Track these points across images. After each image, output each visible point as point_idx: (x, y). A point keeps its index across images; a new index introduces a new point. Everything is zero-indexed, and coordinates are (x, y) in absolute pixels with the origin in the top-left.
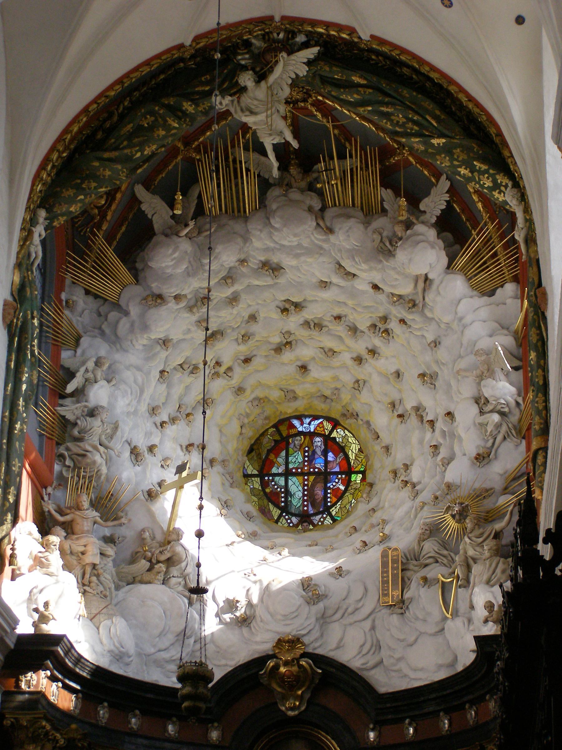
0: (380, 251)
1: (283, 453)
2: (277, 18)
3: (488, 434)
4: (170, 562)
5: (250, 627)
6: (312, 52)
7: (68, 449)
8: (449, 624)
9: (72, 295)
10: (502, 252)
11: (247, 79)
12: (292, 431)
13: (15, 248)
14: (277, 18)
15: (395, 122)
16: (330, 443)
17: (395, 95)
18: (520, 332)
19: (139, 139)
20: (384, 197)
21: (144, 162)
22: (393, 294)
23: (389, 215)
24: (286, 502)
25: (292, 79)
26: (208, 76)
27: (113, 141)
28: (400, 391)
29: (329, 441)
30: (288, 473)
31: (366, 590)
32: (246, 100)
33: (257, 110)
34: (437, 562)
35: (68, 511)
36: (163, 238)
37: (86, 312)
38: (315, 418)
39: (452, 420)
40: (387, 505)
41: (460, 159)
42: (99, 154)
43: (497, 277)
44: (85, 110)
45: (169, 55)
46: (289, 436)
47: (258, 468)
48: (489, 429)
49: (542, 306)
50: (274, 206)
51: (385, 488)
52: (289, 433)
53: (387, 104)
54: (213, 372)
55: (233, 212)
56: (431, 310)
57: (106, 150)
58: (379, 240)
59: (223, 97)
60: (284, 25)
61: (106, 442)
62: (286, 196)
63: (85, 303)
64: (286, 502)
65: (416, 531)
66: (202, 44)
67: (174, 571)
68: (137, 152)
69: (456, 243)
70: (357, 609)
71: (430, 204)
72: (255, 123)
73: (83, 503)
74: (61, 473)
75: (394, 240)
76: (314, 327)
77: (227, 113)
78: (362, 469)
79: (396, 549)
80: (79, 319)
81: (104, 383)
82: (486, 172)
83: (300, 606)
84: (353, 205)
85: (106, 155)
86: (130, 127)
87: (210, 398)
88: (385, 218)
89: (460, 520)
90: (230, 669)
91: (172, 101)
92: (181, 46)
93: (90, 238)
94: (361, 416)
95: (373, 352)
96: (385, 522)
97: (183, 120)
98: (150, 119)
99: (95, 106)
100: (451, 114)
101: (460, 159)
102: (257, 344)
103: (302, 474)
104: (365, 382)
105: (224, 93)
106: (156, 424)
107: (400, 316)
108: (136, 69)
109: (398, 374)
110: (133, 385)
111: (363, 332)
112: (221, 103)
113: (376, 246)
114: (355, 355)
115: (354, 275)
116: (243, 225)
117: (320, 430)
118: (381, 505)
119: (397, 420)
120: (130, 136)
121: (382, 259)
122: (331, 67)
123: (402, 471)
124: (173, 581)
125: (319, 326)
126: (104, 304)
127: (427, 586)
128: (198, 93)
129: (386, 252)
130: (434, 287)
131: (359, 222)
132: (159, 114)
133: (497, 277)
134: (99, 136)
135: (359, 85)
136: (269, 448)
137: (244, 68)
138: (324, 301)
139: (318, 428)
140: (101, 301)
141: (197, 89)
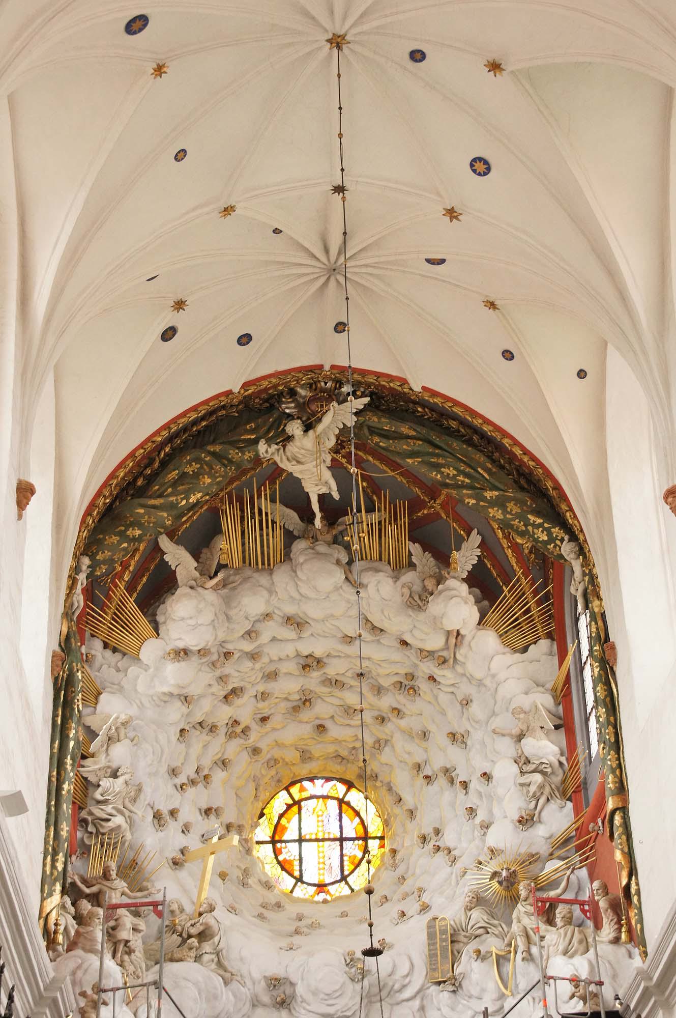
0: (409, 606)
3: (531, 794)
7: (90, 813)
9: (91, 649)
10: (535, 608)
11: (295, 428)
12: (305, 795)
13: (63, 597)
15: (445, 474)
16: (344, 807)
17: (446, 448)
18: (558, 691)
19: (184, 487)
20: (412, 551)
21: (189, 510)
22: (421, 650)
23: (418, 569)
24: (301, 871)
26: (253, 424)
27: (157, 487)
28: (426, 750)
30: (301, 840)
31: (412, 965)
32: (291, 448)
33: (303, 460)
36: (188, 590)
37: (105, 667)
38: (328, 779)
39: (488, 781)
40: (418, 871)
41: (514, 512)
42: (142, 501)
43: (529, 634)
44: (132, 455)
45: (217, 402)
47: (271, 834)
48: (533, 789)
49: (612, 659)
50: (301, 559)
51: (412, 854)
53: (438, 456)
54: (230, 730)
55: (257, 564)
57: (151, 497)
58: (408, 595)
59: (269, 446)
60: (334, 374)
61: (129, 805)
62: (313, 549)
64: (301, 871)
65: (462, 900)
67: (207, 947)
68: (182, 500)
69: (484, 599)
71: (461, 559)
72: (301, 472)
73: (111, 872)
74: (82, 839)
76: (335, 684)
78: (379, 835)
79: (444, 919)
80: (97, 673)
81: (127, 741)
82: (541, 525)
83: (344, 983)
84: (381, 559)
85: (152, 502)
86: (174, 474)
87: (227, 759)
88: (414, 572)
89: (508, 887)
91: (218, 448)
92: (229, 393)
93: (110, 589)
94: (380, 778)
95: (397, 711)
96: (421, 890)
97: (229, 468)
99: (142, 451)
100: (502, 467)
101: (514, 512)
103: (317, 840)
104: (386, 741)
105: (269, 442)
106: (176, 786)
109: (425, 735)
110: (155, 744)
112: (267, 452)
113: (405, 600)
114: (376, 713)
115: (382, 630)
116: (268, 578)
117: (333, 794)
118: (410, 873)
119: (420, 781)
120: (175, 484)
121: (411, 613)
122: (379, 418)
123: (432, 835)
124: (206, 958)
126: (123, 658)
127: (479, 960)
129: (415, 607)
131: (388, 577)
132: (205, 462)
133: (529, 634)
134: (140, 482)
135: (408, 437)
136: (281, 812)
137: (290, 417)
138: (348, 656)
139: (331, 791)
140: (118, 656)
141: (242, 437)
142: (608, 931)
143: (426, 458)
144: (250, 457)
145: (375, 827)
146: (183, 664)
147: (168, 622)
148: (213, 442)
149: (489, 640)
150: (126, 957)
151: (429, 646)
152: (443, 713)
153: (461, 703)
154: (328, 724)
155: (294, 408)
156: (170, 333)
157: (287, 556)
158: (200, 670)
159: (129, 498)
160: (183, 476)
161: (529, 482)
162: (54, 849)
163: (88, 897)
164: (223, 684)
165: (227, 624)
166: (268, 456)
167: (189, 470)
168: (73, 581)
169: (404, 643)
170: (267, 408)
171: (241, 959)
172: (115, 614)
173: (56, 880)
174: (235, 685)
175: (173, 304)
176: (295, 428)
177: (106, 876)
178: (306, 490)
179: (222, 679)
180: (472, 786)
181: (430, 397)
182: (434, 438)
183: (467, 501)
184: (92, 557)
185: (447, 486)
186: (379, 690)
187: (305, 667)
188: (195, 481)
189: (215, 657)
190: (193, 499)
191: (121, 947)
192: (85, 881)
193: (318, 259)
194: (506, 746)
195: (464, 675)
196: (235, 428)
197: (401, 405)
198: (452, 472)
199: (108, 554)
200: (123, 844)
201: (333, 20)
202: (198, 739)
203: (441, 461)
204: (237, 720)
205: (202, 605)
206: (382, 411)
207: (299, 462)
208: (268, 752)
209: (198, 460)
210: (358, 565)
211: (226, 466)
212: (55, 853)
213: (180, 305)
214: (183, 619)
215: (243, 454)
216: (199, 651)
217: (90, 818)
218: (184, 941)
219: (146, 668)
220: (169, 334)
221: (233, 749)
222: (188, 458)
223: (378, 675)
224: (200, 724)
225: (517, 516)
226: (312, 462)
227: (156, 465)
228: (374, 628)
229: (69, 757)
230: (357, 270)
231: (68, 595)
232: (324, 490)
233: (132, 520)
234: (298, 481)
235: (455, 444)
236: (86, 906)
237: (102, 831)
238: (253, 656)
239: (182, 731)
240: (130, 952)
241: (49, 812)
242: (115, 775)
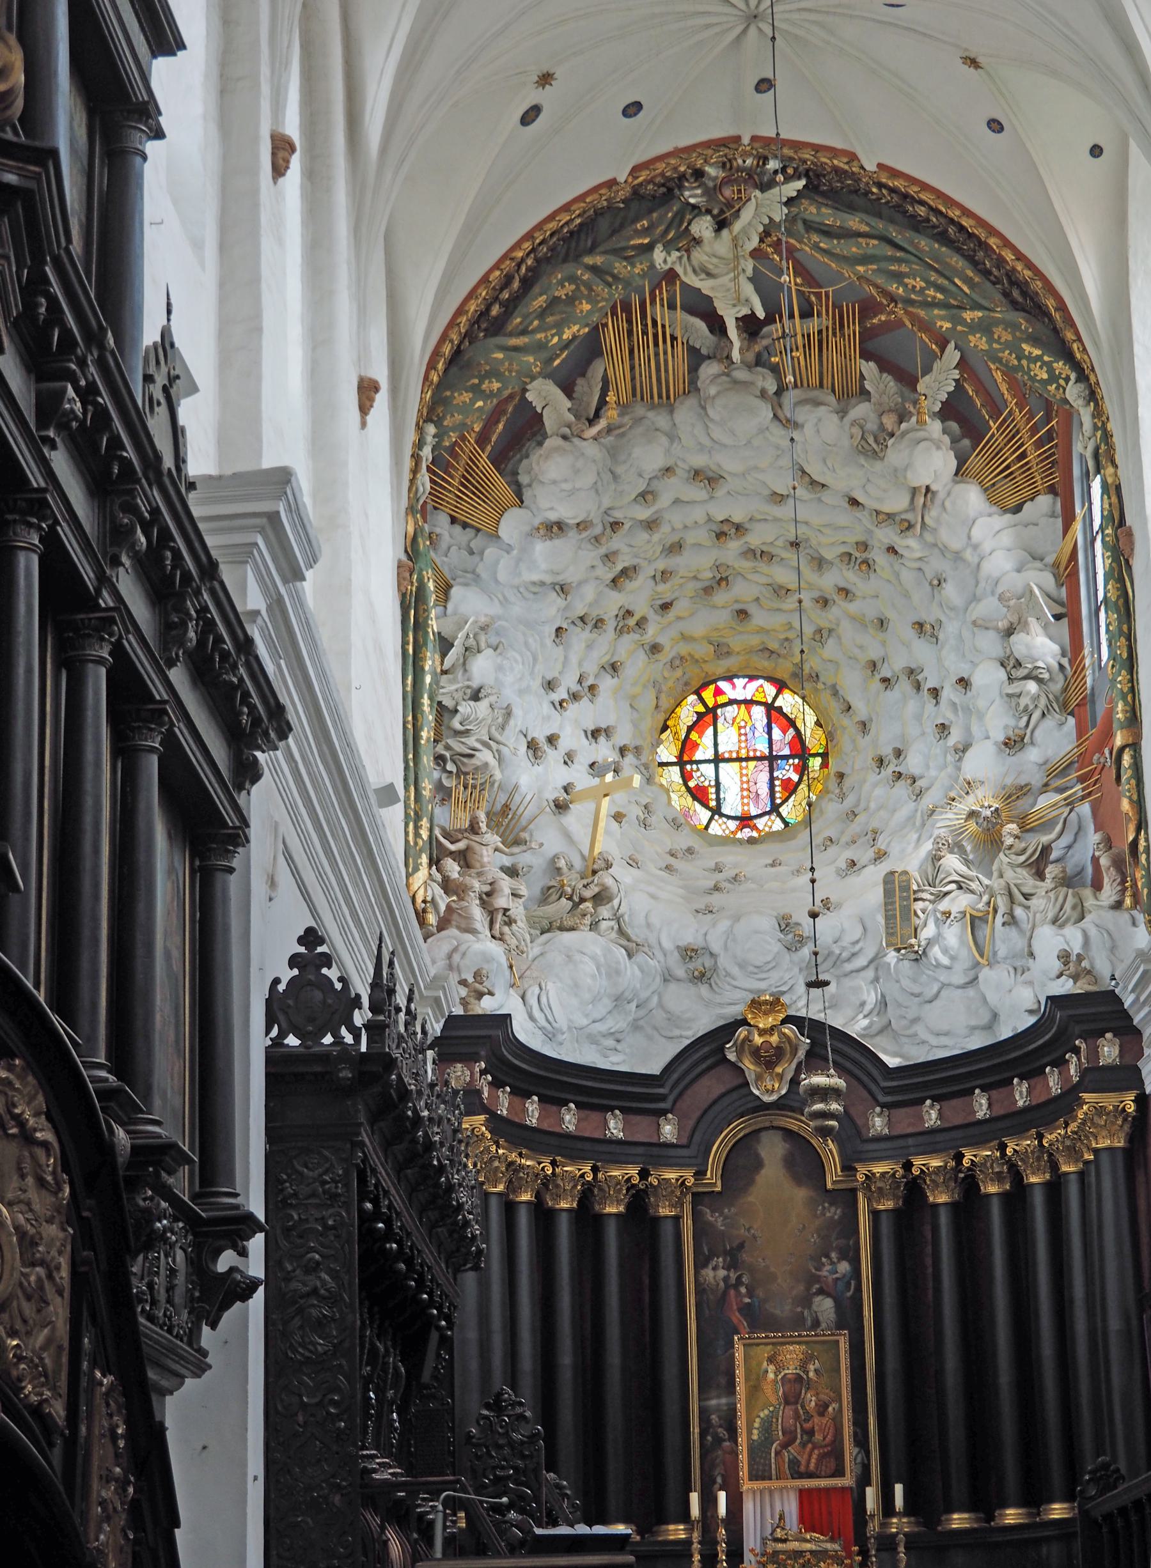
1: (711, 730)
2: (746, 140)
5: (710, 985)
7: (448, 747)
8: (985, 974)
12: (722, 699)
13: (406, 484)
14: (746, 140)
15: (910, 286)
21: (562, 350)
22: (878, 512)
24: (718, 799)
25: (764, 225)
27: (519, 320)
28: (883, 643)
29: (773, 711)
30: (717, 760)
34: (960, 888)
35: (460, 836)
36: (560, 441)
37: (454, 548)
38: (752, 678)
40: (873, 805)
45: (596, 196)
46: (717, 706)
51: (865, 781)
52: (716, 701)
53: (899, 261)
54: (621, 624)
55: (652, 397)
56: (934, 531)
57: (511, 335)
59: (669, 254)
62: (728, 375)
63: (451, 536)
64: (718, 799)
66: (641, 179)
67: (605, 912)
68: (553, 336)
69: (964, 436)
70: (854, 955)
72: (712, 288)
74: (440, 779)
75: (884, 436)
77: (671, 276)
78: (821, 751)
80: (445, 559)
84: (821, 385)
90: (688, 1042)
91: (597, 260)
92: (612, 183)
94: (822, 679)
95: (845, 592)
98: (569, 288)
99: (497, 273)
102: (682, 581)
103: (739, 759)
105: (668, 247)
107: (887, 541)
108: (551, 217)
109: (882, 623)
111: (832, 564)
112: (665, 261)
114: (816, 594)
115: (823, 486)
116: (668, 418)
117: (759, 697)
118: (863, 805)
119: (876, 684)
120: (542, 313)
122: (818, 209)
123: (892, 757)
124: (604, 925)
125: (764, 555)
128: (634, 247)
130: (938, 501)
132: (582, 281)
134: (495, 310)
136: (690, 724)
138: (776, 520)
140: (470, 532)
141: (632, 243)
143: (883, 265)
144: (642, 270)
145: (814, 739)
146: (557, 542)
147: (534, 485)
148: (591, 251)
149: (972, 497)
150: (506, 929)
151: (887, 509)
152: (907, 595)
153: (931, 584)
154: (752, 609)
155: (702, 195)
156: (532, 114)
158: (579, 548)
159: (482, 334)
160: (554, 302)
161: (1024, 294)
162: (416, 813)
164: (610, 564)
165: (613, 487)
166: (667, 267)
167: (561, 293)
168: (416, 458)
169: (854, 502)
170: (664, 194)
171: (649, 925)
172: (464, 477)
173: (421, 851)
174: (626, 564)
175: (536, 79)
177: (474, 828)
178: (720, 312)
179: (608, 558)
181: (889, 178)
183: (939, 324)
184: (438, 424)
185: (912, 302)
187: (720, 535)
188: (568, 309)
189: (598, 530)
191: (499, 917)
192: (447, 835)
193: (735, 6)
195: (935, 545)
196: (622, 226)
197: (849, 185)
199: (458, 417)
200: (492, 784)
202: (579, 637)
203: (904, 268)
204: (631, 609)
205: (580, 464)
206: (823, 194)
207: (709, 275)
208: (672, 647)
209: (572, 279)
210: (791, 396)
211: (610, 285)
212: (418, 818)
213: (545, 79)
214: (554, 482)
215: (633, 265)
216: (578, 524)
217: (448, 755)
218: (576, 905)
219: (509, 549)
220: (530, 116)
221: (627, 648)
222: (560, 276)
223: (819, 544)
224: (582, 619)
226: (727, 273)
227: (516, 285)
228: (813, 482)
229: (426, 696)
230: (787, 16)
231: (412, 481)
232: (745, 311)
233: (488, 368)
234: (710, 299)
235: (923, 243)
236: (453, 868)
237: (463, 769)
238: (650, 525)
239: (559, 630)
240: (510, 922)
241: (406, 768)
242: (476, 696)
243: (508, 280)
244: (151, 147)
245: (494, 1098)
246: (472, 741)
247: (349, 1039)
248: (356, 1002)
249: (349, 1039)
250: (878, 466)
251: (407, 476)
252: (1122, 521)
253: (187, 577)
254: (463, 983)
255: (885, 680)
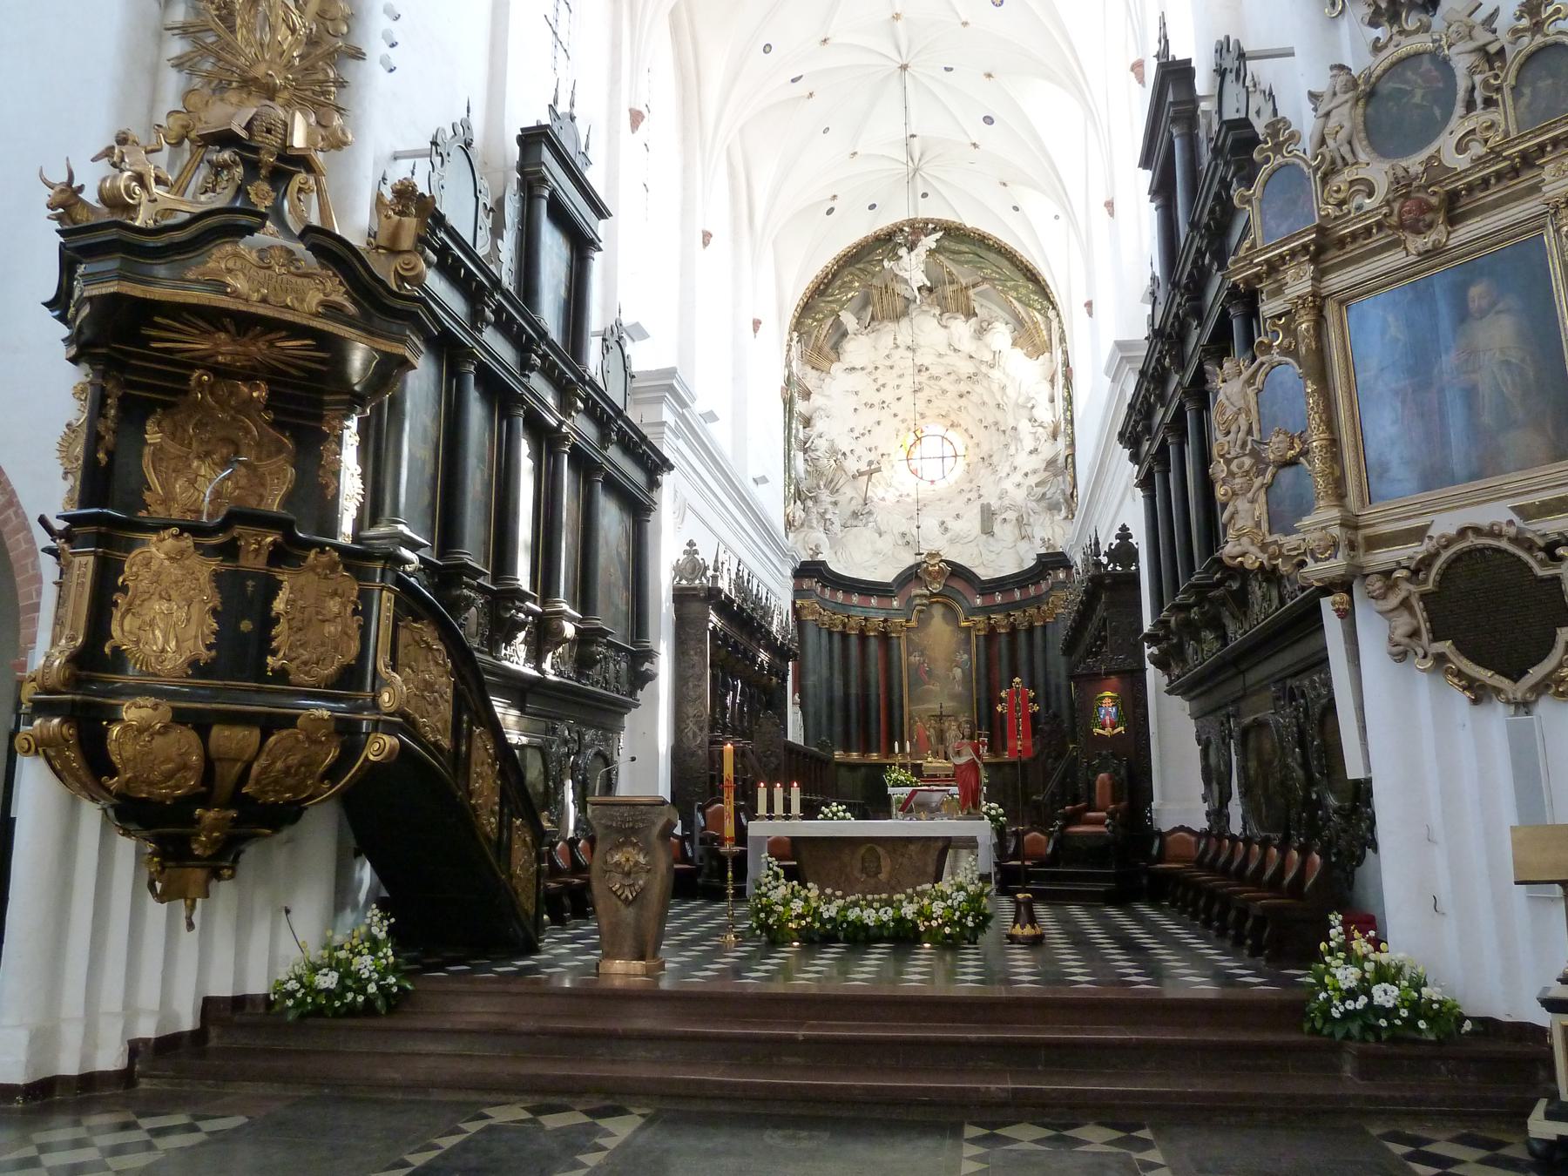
4: (870, 513)
6: (939, 235)
12: (923, 434)
42: (823, 298)
50: (914, 314)
53: (981, 262)
67: (871, 519)
85: (830, 299)
86: (839, 283)
91: (861, 266)
100: (1017, 266)
124: (870, 525)
142: (1063, 513)
145: (961, 451)
149: (1019, 353)
154: (933, 399)
157: (905, 313)
163: (811, 498)
169: (971, 357)
176: (903, 252)
177: (818, 486)
179: (875, 380)
180: (1007, 432)
182: (979, 251)
186: (958, 381)
187: (920, 371)
190: (850, 296)
194: (1025, 413)
198: (989, 271)
201: (901, 57)
202: (864, 411)
209: (851, 274)
210: (947, 315)
212: (789, 485)
220: (830, 211)
225: (1024, 295)
228: (955, 350)
236: (810, 503)
239: (856, 410)
243: (827, 274)
244: (596, 255)
245: (822, 592)
246: (818, 453)
247: (705, 581)
248: (706, 568)
249: (705, 581)
250: (980, 343)
251: (785, 353)
252: (1068, 366)
253: (609, 417)
254: (811, 549)
255: (986, 427)
